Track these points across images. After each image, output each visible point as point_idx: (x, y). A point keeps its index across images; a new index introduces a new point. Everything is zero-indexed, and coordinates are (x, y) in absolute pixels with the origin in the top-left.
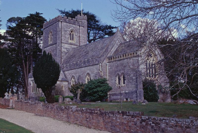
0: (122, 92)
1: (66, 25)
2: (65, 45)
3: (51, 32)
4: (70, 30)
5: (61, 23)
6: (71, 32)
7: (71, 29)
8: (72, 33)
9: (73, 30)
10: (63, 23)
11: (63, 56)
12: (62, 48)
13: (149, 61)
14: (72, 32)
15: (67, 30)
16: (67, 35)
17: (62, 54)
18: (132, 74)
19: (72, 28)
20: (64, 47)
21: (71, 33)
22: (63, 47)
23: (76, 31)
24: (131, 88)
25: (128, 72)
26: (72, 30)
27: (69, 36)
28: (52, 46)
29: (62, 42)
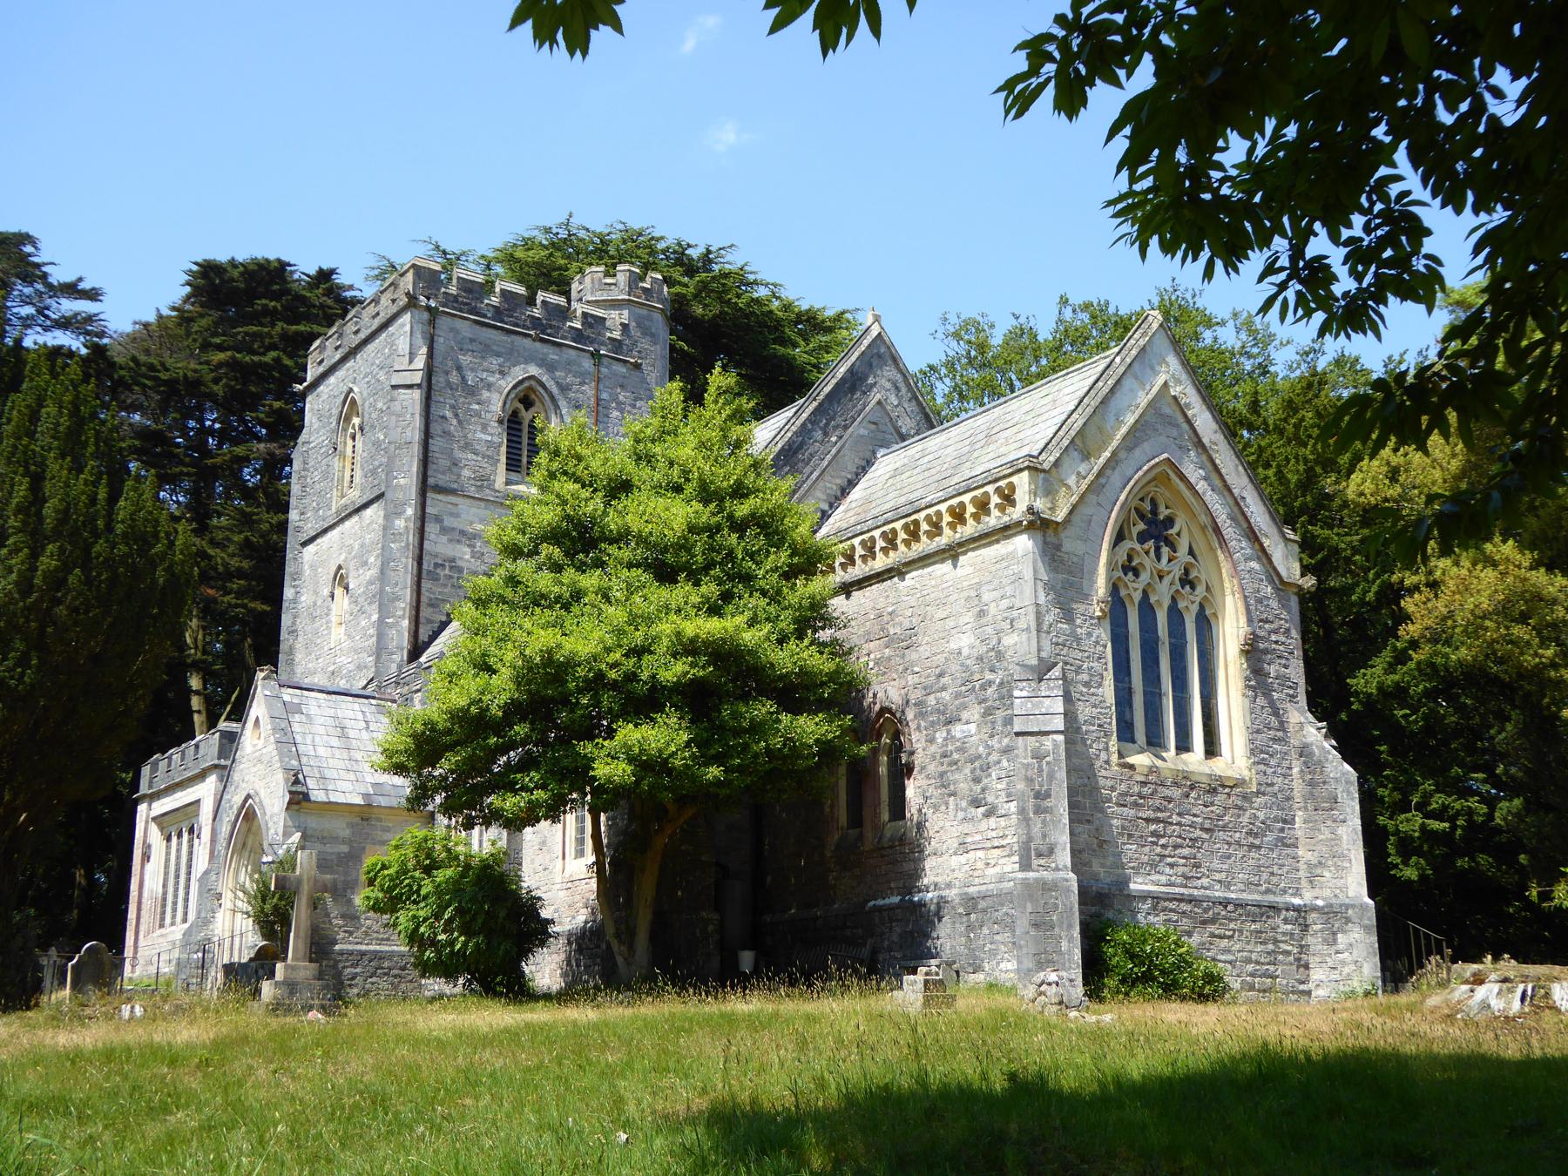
0: (880, 902)
1: (472, 340)
2: (454, 510)
3: (354, 402)
4: (507, 384)
5: (432, 322)
6: (521, 407)
7: (518, 373)
8: (526, 416)
9: (533, 383)
10: (443, 322)
11: (432, 605)
12: (432, 529)
13: (1145, 577)
14: (527, 402)
15: (489, 386)
16: (484, 428)
17: (425, 585)
18: (965, 715)
19: (533, 370)
20: (449, 522)
21: (515, 413)
22: (438, 519)
23: (569, 401)
24: (963, 859)
25: (931, 700)
26: (530, 388)
27: (496, 439)
28: (355, 519)
29: (431, 481)
